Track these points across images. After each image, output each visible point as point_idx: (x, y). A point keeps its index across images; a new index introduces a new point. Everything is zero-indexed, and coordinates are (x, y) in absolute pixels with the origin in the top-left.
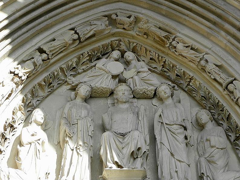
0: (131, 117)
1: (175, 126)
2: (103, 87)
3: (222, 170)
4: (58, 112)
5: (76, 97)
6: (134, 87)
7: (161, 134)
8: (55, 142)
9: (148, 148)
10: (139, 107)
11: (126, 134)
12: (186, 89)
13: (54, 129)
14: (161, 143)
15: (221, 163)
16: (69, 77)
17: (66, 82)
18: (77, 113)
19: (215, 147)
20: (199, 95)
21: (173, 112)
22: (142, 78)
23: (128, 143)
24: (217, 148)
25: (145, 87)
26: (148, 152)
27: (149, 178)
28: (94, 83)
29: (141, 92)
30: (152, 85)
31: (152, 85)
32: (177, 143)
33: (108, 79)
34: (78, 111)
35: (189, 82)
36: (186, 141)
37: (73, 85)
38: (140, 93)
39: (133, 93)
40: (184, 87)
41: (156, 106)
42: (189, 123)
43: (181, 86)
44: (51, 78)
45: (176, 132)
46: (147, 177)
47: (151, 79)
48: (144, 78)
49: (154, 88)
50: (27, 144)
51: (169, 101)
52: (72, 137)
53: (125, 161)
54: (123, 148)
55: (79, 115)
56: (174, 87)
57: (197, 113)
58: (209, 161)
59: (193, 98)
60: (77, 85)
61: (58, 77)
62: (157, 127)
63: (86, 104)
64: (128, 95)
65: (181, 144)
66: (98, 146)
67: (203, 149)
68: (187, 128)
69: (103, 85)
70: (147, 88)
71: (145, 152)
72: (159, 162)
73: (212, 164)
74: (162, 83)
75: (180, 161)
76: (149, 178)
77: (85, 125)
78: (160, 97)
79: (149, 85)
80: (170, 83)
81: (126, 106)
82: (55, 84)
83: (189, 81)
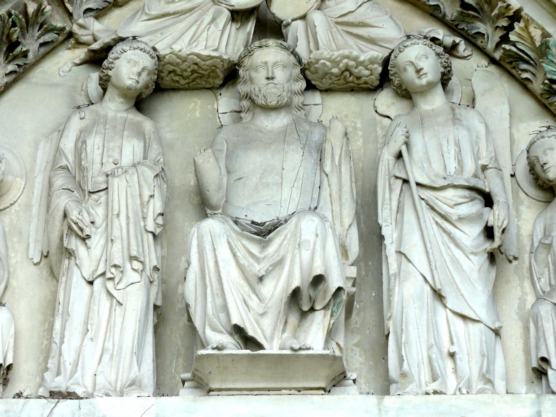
0: (295, 160)
1: (450, 193)
2: (198, 56)
4: (41, 146)
5: (105, 90)
6: (311, 52)
7: (399, 222)
9: (353, 272)
10: (326, 123)
11: (275, 226)
12: (497, 55)
13: (28, 206)
14: (400, 253)
16: (81, 21)
17: (71, 35)
18: (108, 151)
20: (540, 77)
21: (444, 142)
22: (340, 20)
23: (279, 263)
25: (346, 52)
26: (354, 289)
27: (354, 381)
28: (167, 41)
29: (335, 71)
30: (372, 41)
31: (372, 41)
32: (457, 253)
33: (217, 26)
34: (111, 145)
35: (510, 28)
36: (489, 246)
37: (96, 46)
38: (332, 74)
39: (307, 72)
40: (490, 46)
41: (388, 117)
42: (502, 179)
43: (479, 43)
44: (14, 25)
45: (454, 213)
46: (349, 375)
47: (368, 21)
48: (345, 19)
49: (380, 54)
51: (436, 101)
52: (89, 237)
53: (267, 322)
55: (111, 160)
56: (455, 46)
57: (532, 144)
59: (524, 85)
60: (107, 48)
61: (41, 20)
62: (387, 196)
63: (138, 117)
64: (288, 81)
65: (471, 257)
66: (183, 265)
67: (549, 271)
68: (495, 199)
69: (201, 49)
70: (355, 53)
71: (339, 289)
72: (390, 324)
74: (408, 37)
75: (464, 317)
76: (354, 381)
77: (132, 195)
78: (404, 87)
79: (362, 43)
80: (441, 33)
81: (277, 122)
82: (31, 44)
83: (505, 24)
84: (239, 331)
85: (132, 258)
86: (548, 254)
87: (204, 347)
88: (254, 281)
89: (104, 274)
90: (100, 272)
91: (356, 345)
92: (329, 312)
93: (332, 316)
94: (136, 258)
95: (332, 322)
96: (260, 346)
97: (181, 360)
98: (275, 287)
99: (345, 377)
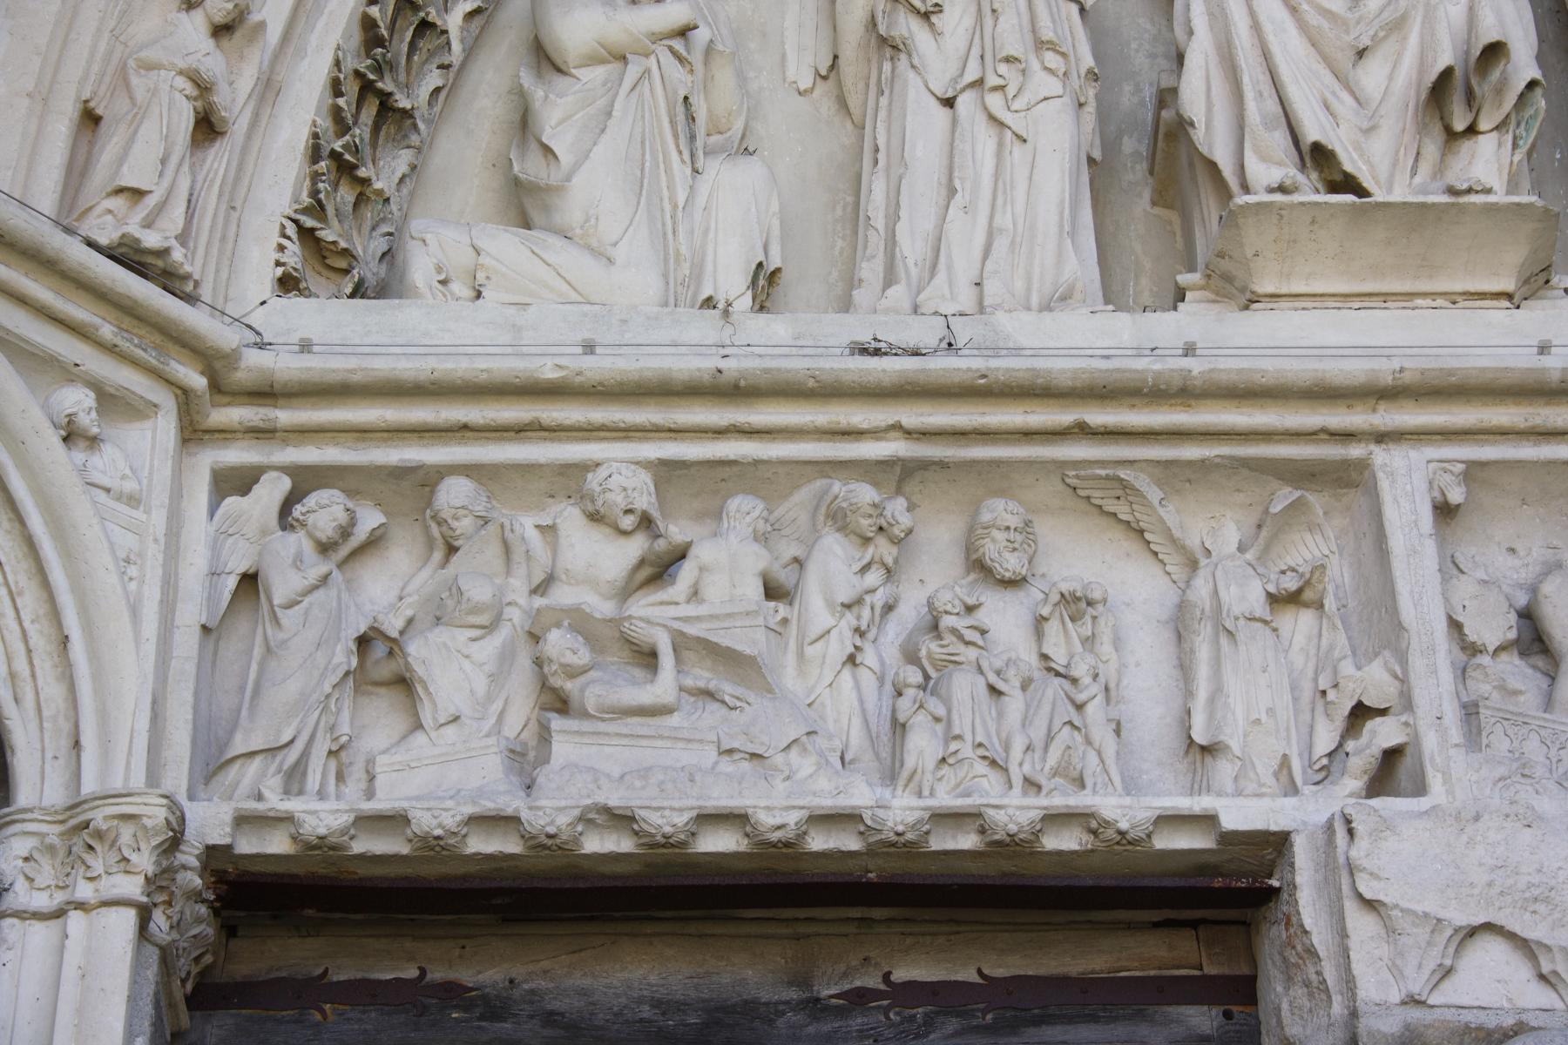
8: (791, 73)
50: (593, 60)
71: (1532, 85)
84: (1319, 157)
85: (1041, 45)
88: (1345, 59)
89: (979, 83)
90: (970, 76)
92: (1509, 138)
93: (1515, 146)
94: (1052, 46)
97: (1144, 281)
98: (1391, 78)
99: (1547, 282)
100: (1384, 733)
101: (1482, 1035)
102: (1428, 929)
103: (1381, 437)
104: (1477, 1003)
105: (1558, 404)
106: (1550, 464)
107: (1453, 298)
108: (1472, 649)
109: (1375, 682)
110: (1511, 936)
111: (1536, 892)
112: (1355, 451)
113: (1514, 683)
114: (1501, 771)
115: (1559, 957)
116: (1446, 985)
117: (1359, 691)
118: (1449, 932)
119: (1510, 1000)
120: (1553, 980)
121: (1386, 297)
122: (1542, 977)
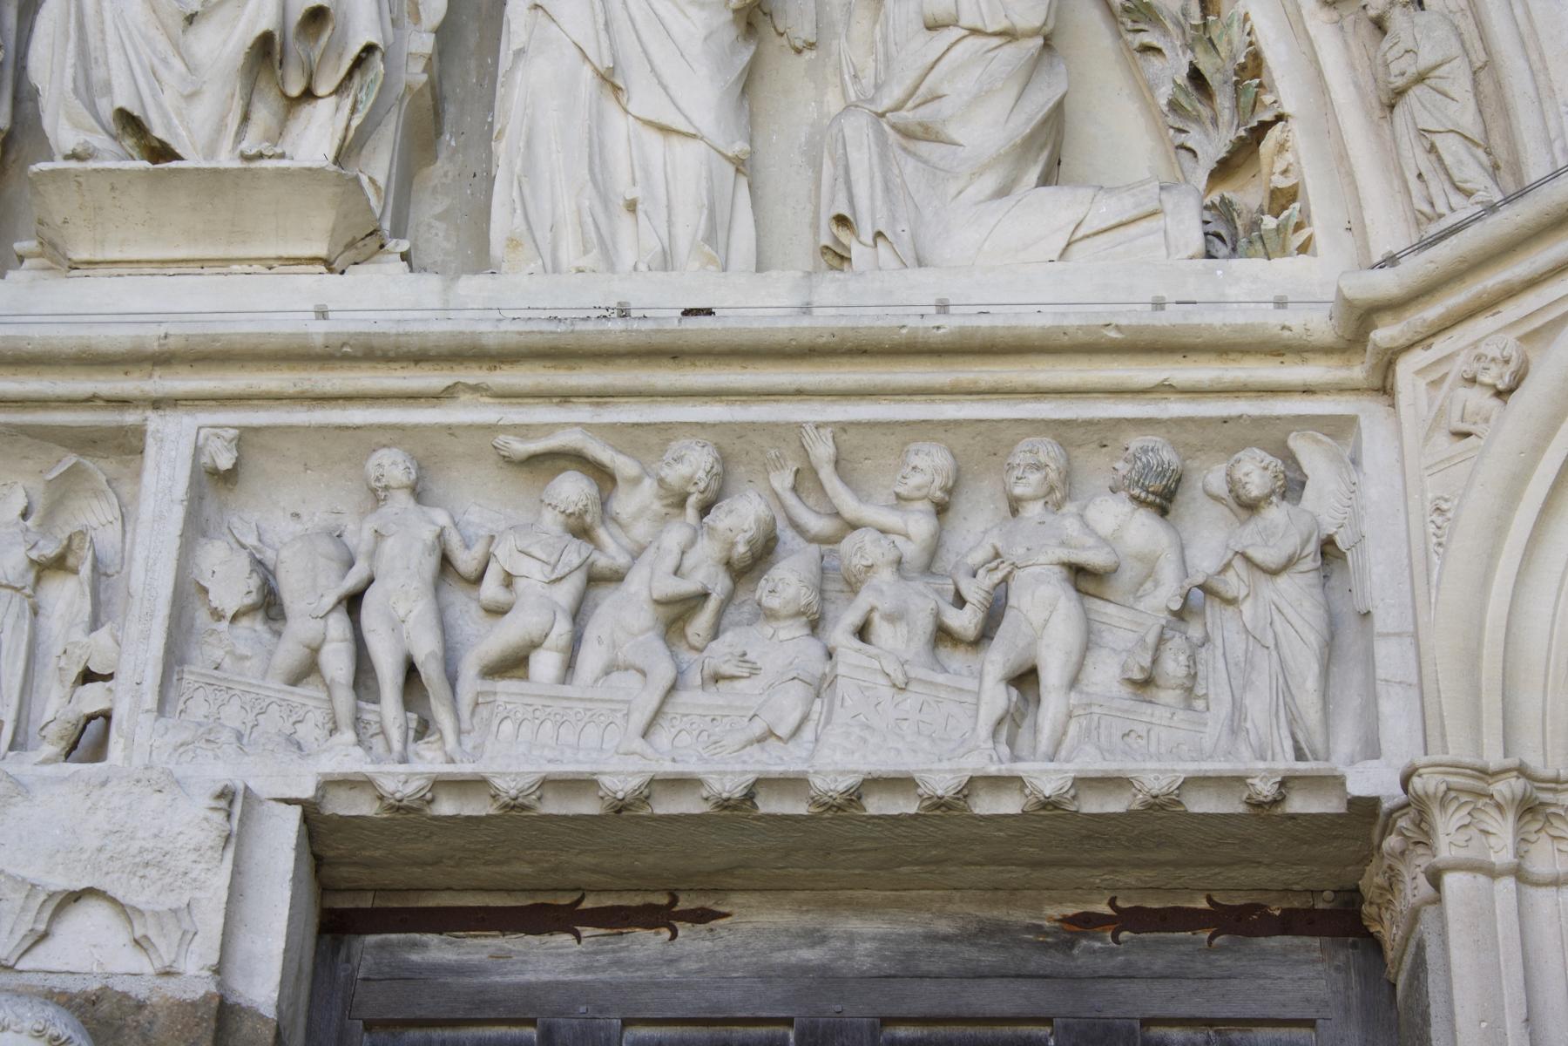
3: (989, 182)
15: (986, 123)
19: (955, 23)
24: (974, 32)
53: (203, 113)
54: (191, 19)
58: (906, 133)
71: (370, 49)
73: (923, 148)
75: (665, 130)
84: (130, 123)
86: (875, 22)
87: (51, 159)
88: (176, 24)
91: (439, 217)
92: (347, 103)
95: (356, 122)
96: (178, 157)
98: (225, 43)
99: (382, 246)
100: (93, 698)
101: (64, 999)
102: (24, 894)
103: (157, 404)
104: (66, 968)
105: (332, 369)
106: (321, 428)
107: (269, 263)
108: (217, 615)
109: (99, 649)
110: (114, 901)
111: (148, 857)
112: (131, 418)
113: (243, 649)
114: (186, 736)
115: (151, 921)
116: (40, 950)
117: (85, 658)
118: (42, 897)
119: (100, 964)
120: (145, 944)
121: (203, 262)
122: (136, 942)
